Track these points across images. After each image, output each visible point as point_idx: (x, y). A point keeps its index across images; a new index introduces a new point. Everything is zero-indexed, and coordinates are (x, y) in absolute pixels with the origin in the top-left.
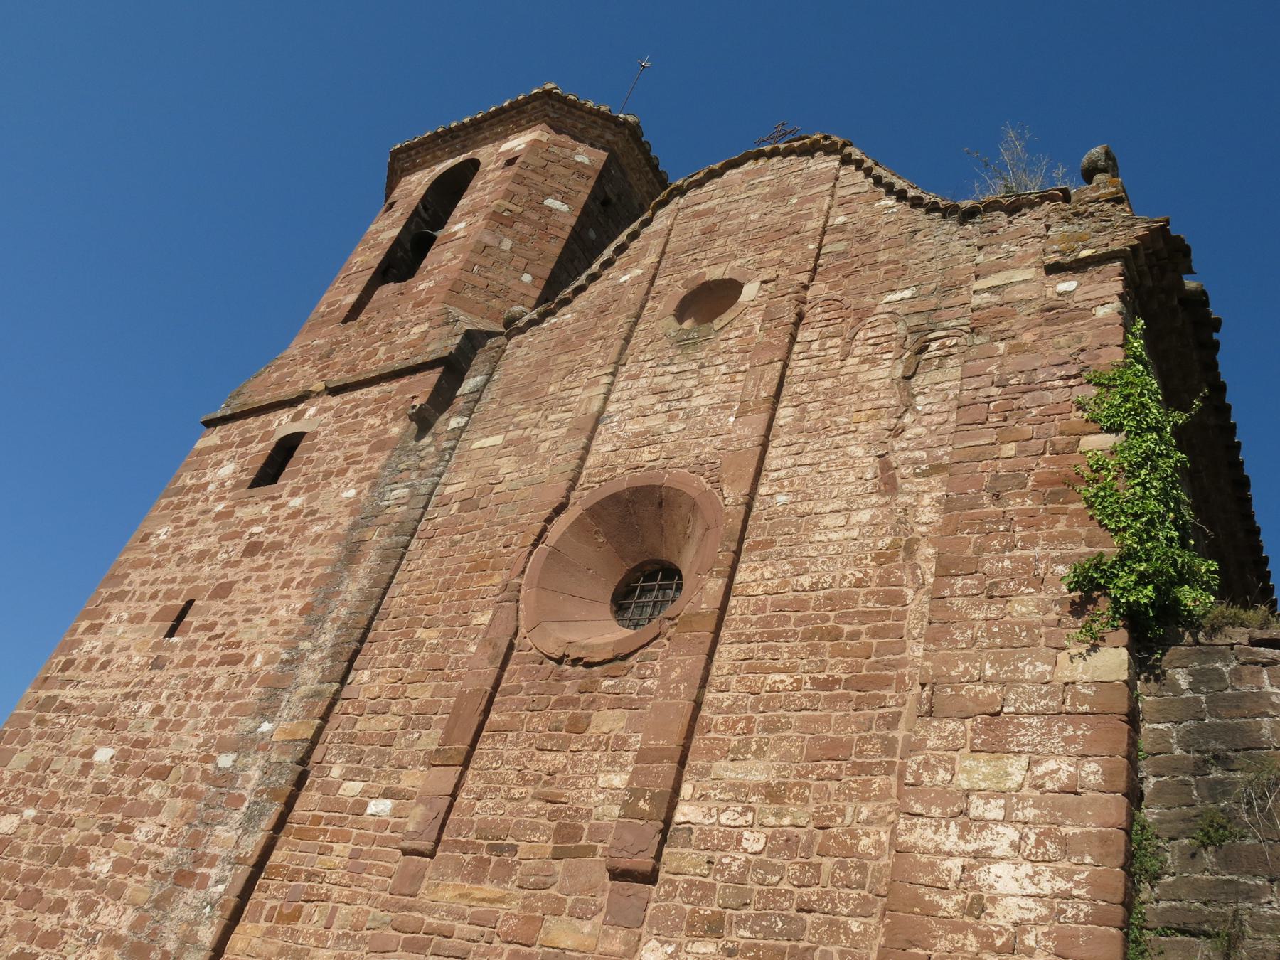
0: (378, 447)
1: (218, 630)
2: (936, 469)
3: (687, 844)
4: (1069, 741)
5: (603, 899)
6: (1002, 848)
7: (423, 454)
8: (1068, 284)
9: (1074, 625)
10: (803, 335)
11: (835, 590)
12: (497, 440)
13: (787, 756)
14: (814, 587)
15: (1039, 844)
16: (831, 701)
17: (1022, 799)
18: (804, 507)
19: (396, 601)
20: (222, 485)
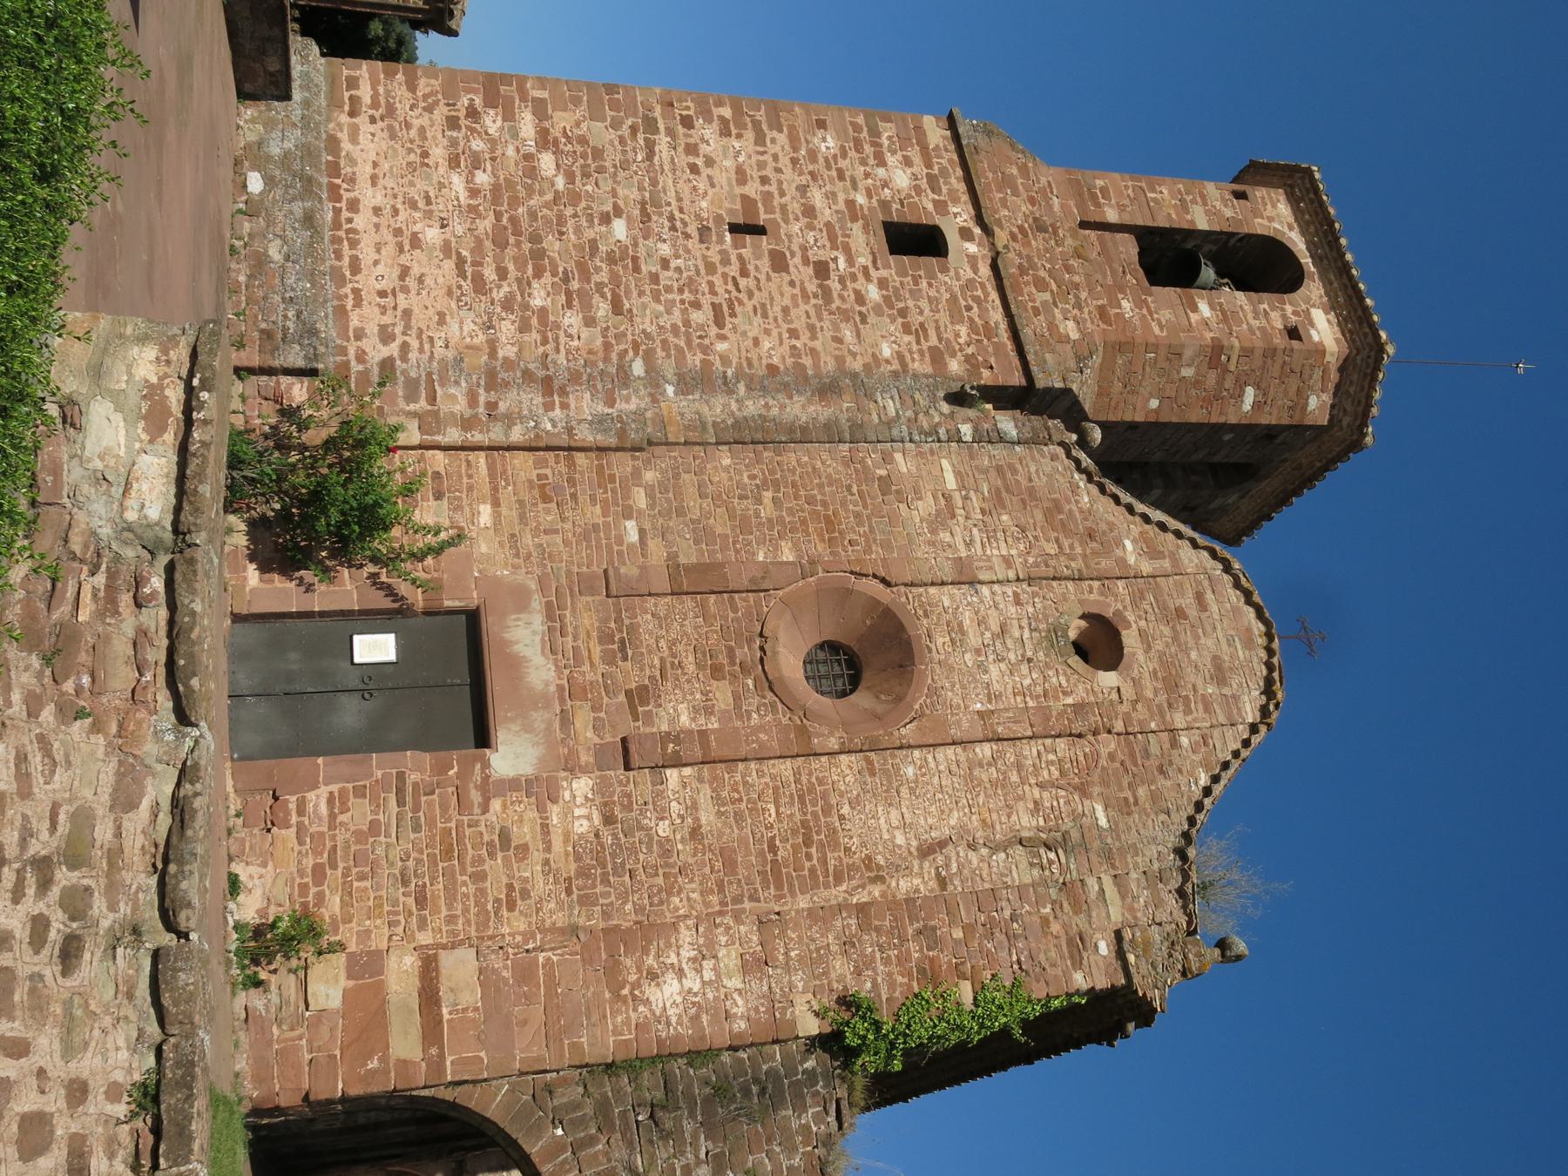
0: (937, 357)
1: (743, 282)
2: (942, 882)
3: (654, 784)
4: (756, 1010)
5: (608, 738)
6: (687, 983)
7: (932, 411)
8: (1103, 948)
9: (828, 1001)
10: (1061, 744)
11: (841, 834)
12: (951, 482)
13: (721, 834)
14: (842, 818)
15: (694, 1003)
16: (761, 854)
17: (717, 989)
18: (904, 791)
19: (794, 457)
20: (885, 184)
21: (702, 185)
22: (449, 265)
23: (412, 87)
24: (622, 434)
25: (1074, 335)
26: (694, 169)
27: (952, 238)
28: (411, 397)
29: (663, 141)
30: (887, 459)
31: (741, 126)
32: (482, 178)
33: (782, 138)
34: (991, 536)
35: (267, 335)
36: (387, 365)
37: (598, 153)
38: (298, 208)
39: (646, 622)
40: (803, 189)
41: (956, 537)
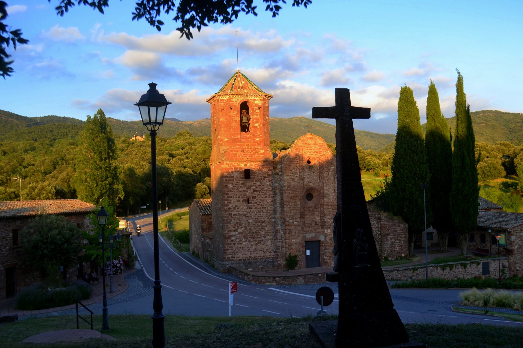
12: (288, 177)
21: (241, 208)
22: (259, 244)
23: (228, 250)
24: (283, 223)
25: (263, 151)
26: (238, 208)
27: (246, 168)
28: (279, 249)
29: (233, 213)
30: (285, 186)
31: (229, 200)
32: (244, 240)
33: (230, 193)
34: (295, 173)
35: (273, 267)
36: (275, 252)
37: (237, 223)
38: (253, 264)
39: (307, 222)
40: (240, 191)
41: (297, 179)
